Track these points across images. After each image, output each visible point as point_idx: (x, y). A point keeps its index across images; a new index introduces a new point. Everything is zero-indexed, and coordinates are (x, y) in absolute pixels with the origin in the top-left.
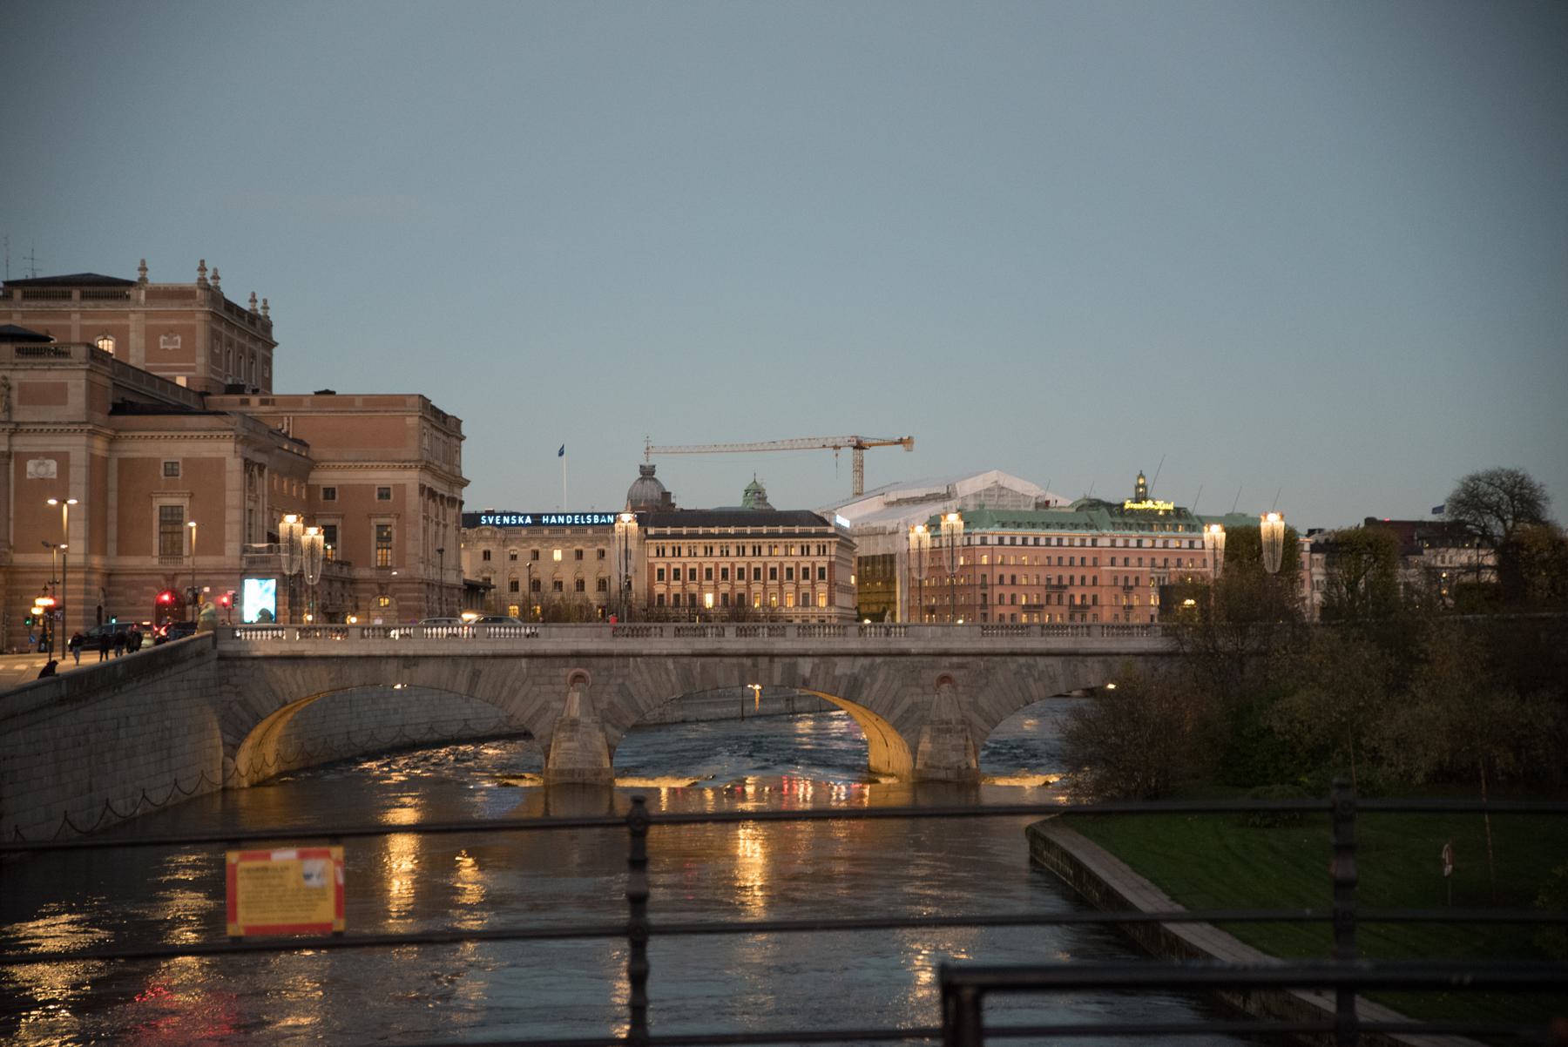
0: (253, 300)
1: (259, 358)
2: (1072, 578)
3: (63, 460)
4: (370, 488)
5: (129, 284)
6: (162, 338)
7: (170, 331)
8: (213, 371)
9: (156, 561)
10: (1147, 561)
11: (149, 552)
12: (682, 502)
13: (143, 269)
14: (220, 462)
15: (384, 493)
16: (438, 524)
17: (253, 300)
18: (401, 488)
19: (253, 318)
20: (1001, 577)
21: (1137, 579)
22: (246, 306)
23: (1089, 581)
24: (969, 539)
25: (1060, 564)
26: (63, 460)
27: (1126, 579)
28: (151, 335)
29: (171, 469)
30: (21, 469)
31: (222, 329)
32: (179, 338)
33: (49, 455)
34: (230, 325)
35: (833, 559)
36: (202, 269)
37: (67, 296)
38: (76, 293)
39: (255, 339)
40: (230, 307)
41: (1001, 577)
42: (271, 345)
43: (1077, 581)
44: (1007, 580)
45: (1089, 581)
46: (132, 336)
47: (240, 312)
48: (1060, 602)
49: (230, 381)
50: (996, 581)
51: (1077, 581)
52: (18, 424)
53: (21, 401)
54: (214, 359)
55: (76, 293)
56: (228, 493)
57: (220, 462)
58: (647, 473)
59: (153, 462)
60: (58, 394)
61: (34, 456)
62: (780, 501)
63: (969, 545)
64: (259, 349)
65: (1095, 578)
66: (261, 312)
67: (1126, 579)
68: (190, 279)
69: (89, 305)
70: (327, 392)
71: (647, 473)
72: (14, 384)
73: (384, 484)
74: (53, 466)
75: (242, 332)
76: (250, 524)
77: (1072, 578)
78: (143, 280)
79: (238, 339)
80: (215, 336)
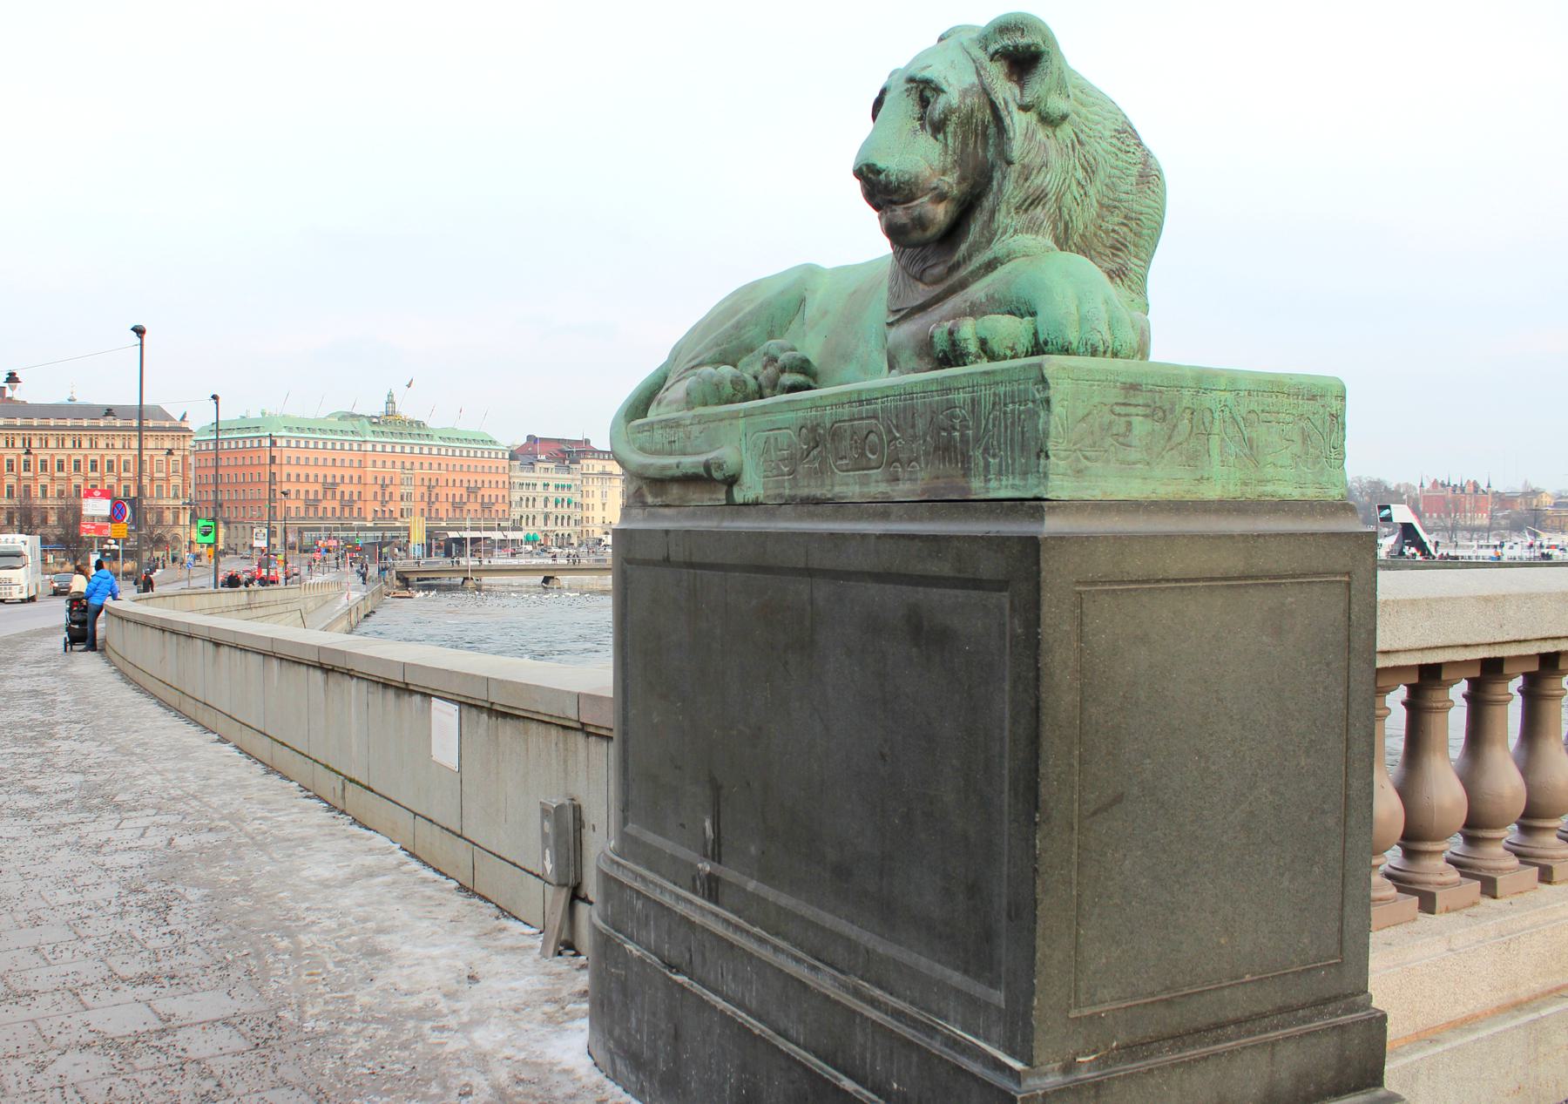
2: (343, 477)
10: (398, 464)
20: (289, 475)
21: (437, 480)
23: (355, 480)
24: (260, 441)
25: (334, 464)
27: (384, 479)
35: (186, 453)
41: (289, 475)
43: (347, 480)
44: (293, 478)
45: (355, 480)
48: (334, 498)
50: (284, 479)
51: (347, 480)
62: (81, 399)
63: (260, 446)
65: (360, 477)
67: (384, 479)
77: (343, 477)
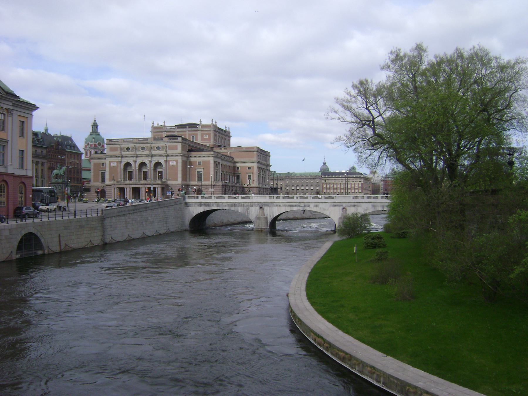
0: (226, 128)
1: (227, 139)
3: (177, 161)
4: (246, 167)
5: (198, 125)
6: (204, 136)
7: (206, 134)
8: (215, 143)
9: (196, 183)
11: (195, 181)
12: (331, 170)
13: (201, 121)
14: (209, 162)
15: (249, 168)
16: (263, 175)
17: (226, 128)
18: (253, 167)
19: (225, 131)
22: (224, 129)
26: (177, 161)
28: (202, 135)
29: (199, 162)
30: (169, 163)
31: (217, 134)
32: (208, 136)
33: (174, 160)
34: (219, 133)
36: (212, 121)
37: (186, 128)
38: (187, 127)
39: (226, 136)
40: (219, 129)
42: (230, 137)
46: (198, 135)
47: (222, 130)
49: (219, 145)
52: (168, 154)
53: (169, 149)
54: (215, 140)
55: (187, 127)
56: (211, 168)
57: (209, 162)
58: (324, 164)
59: (196, 162)
60: (176, 148)
61: (171, 161)
64: (227, 138)
66: (228, 130)
68: (209, 123)
69: (190, 129)
70: (240, 147)
71: (324, 164)
72: (167, 146)
73: (249, 166)
74: (175, 162)
75: (222, 134)
76: (216, 175)
78: (201, 123)
79: (221, 136)
80: (215, 135)
